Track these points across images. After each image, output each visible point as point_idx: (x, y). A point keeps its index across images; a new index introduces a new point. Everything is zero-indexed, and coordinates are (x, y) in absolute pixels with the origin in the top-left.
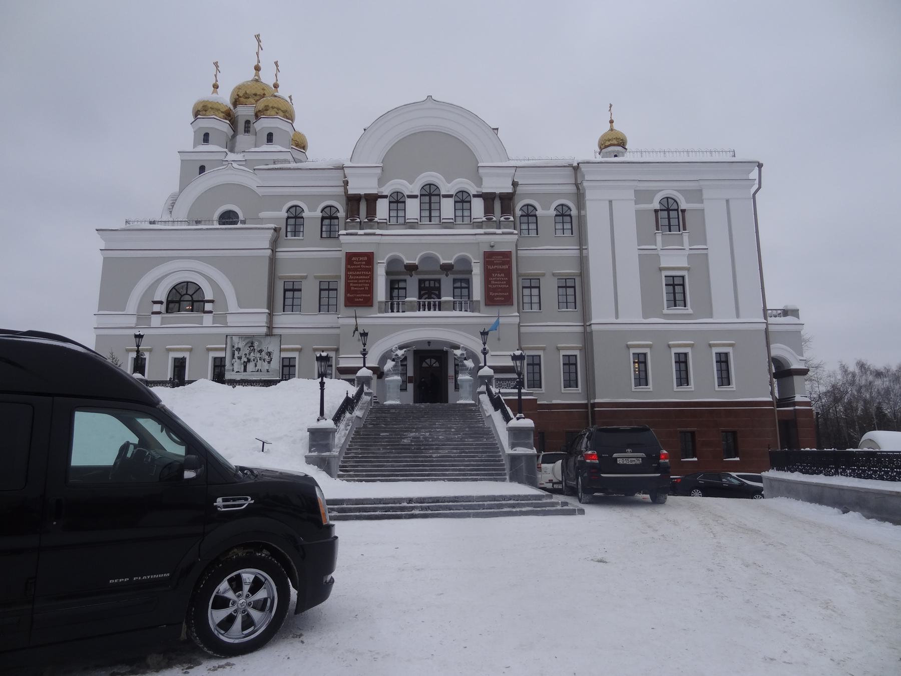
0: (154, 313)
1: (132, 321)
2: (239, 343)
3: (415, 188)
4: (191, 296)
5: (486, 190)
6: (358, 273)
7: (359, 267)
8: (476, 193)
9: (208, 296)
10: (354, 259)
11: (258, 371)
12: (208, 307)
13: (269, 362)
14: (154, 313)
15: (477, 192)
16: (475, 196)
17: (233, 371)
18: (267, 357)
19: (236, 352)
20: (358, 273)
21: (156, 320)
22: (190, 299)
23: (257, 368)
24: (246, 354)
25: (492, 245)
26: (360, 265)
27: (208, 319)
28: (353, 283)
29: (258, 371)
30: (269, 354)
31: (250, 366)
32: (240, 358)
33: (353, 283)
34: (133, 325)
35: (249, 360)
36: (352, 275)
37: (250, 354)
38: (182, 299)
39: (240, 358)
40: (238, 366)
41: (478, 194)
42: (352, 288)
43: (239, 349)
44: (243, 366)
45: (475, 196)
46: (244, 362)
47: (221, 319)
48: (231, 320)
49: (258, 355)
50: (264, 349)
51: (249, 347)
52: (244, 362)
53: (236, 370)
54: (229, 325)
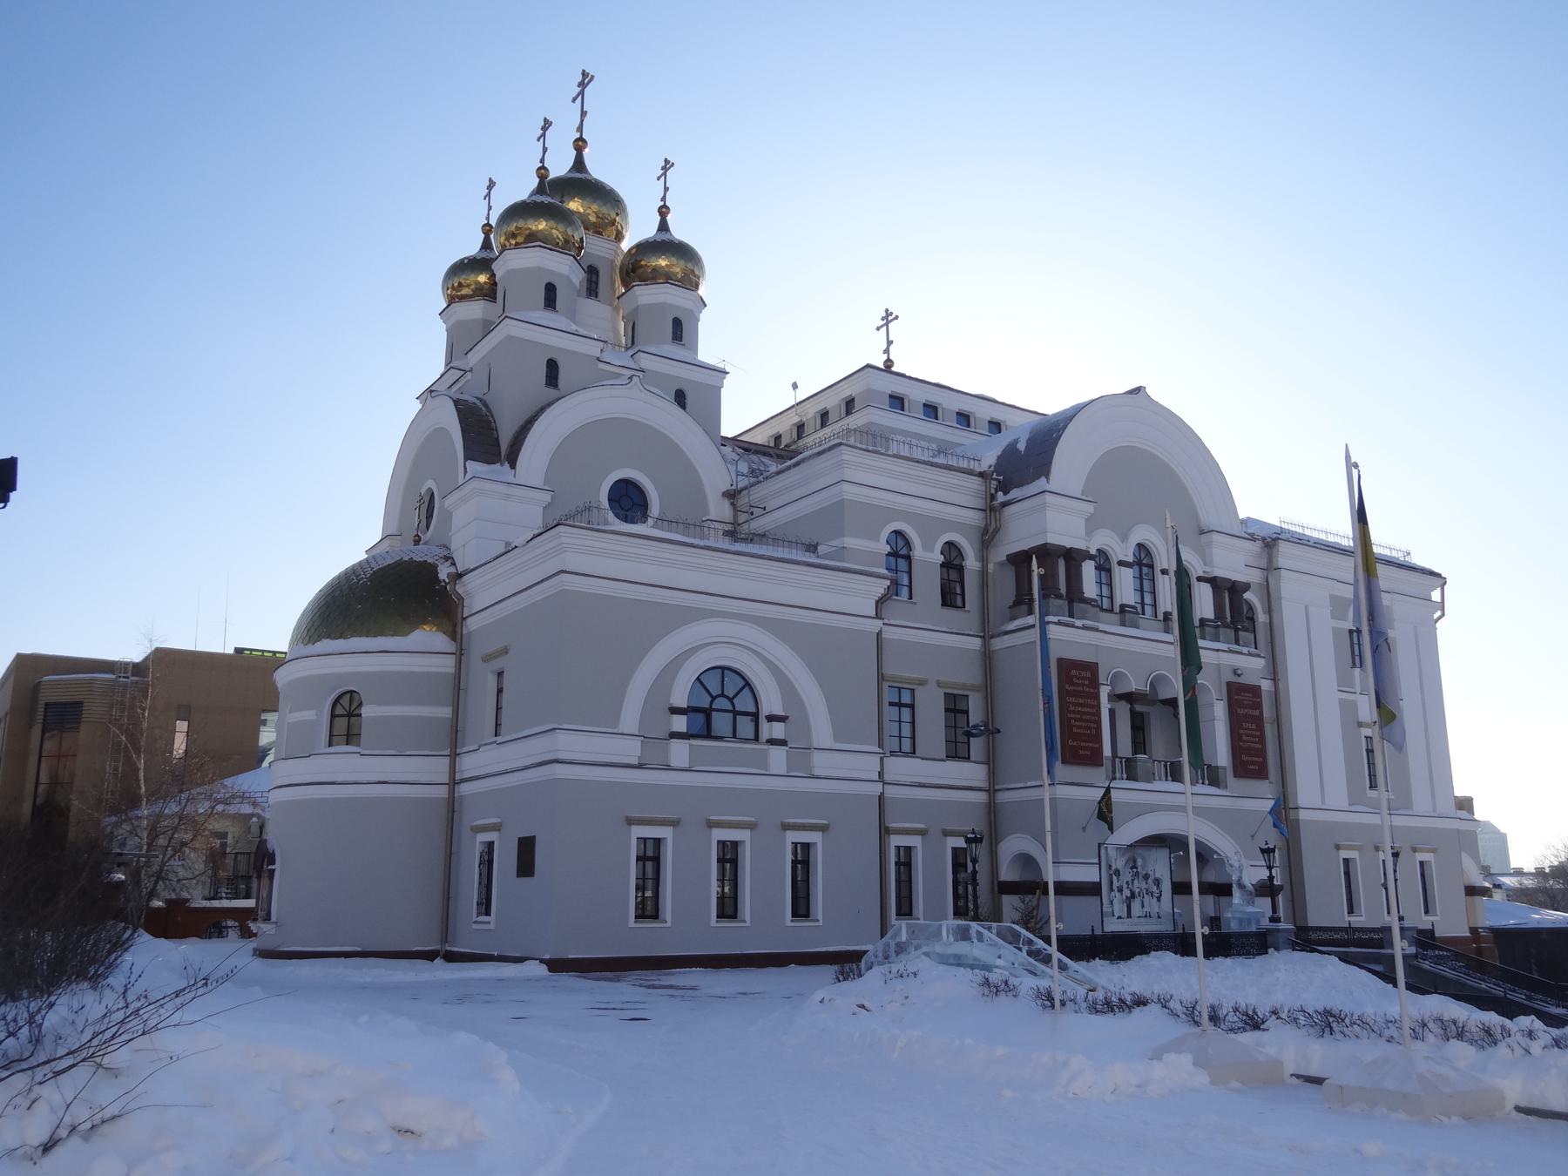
0: (675, 735)
1: (631, 750)
2: (1116, 860)
3: (1123, 551)
4: (731, 700)
5: (1219, 573)
6: (1081, 701)
7: (1080, 689)
8: (1202, 574)
9: (771, 703)
10: (1073, 672)
11: (1146, 916)
12: (778, 730)
13: (1159, 899)
14: (675, 735)
15: (1204, 572)
16: (1199, 579)
17: (1113, 915)
18: (1154, 889)
19: (1115, 878)
20: (1081, 701)
21: (679, 752)
22: (731, 708)
23: (1145, 909)
24: (1127, 882)
25: (1239, 672)
26: (1083, 685)
27: (777, 756)
28: (1076, 720)
29: (1146, 916)
30: (1157, 882)
31: (1136, 905)
32: (1120, 890)
33: (1076, 720)
34: (635, 761)
35: (1133, 896)
36: (1074, 704)
37: (1133, 880)
38: (713, 707)
39: (1120, 890)
40: (1120, 909)
41: (1206, 576)
42: (1075, 730)
43: (1117, 872)
44: (1125, 904)
45: (1199, 579)
46: (1127, 897)
47: (801, 765)
48: (822, 763)
49: (1144, 885)
50: (1150, 872)
51: (1131, 868)
52: (1127, 897)
53: (1117, 914)
54: (816, 773)
